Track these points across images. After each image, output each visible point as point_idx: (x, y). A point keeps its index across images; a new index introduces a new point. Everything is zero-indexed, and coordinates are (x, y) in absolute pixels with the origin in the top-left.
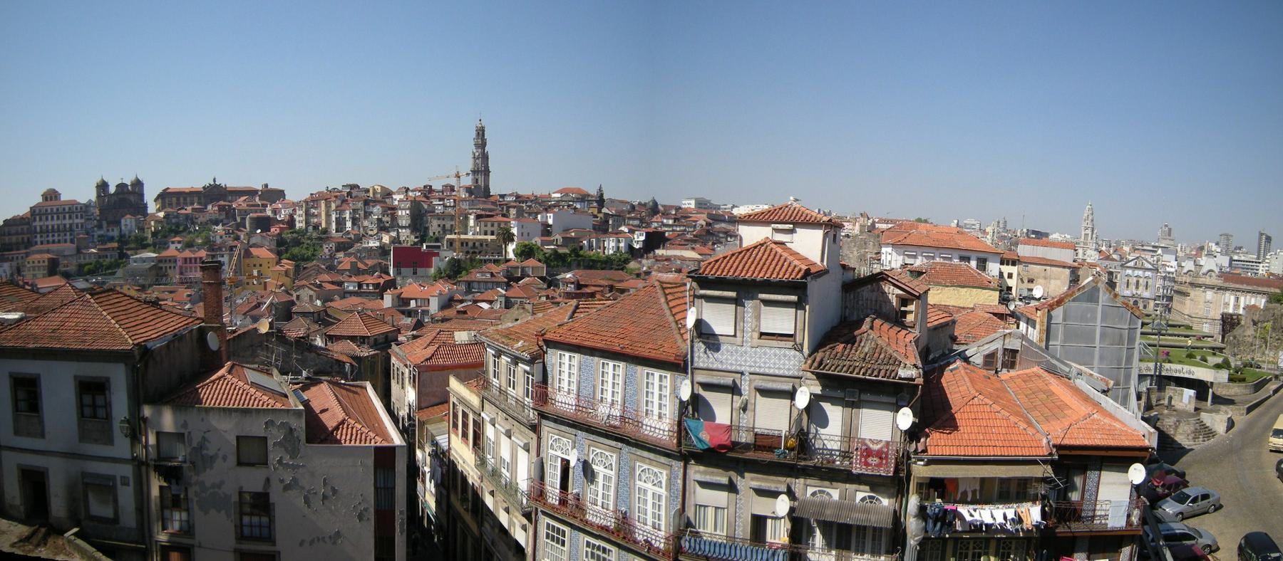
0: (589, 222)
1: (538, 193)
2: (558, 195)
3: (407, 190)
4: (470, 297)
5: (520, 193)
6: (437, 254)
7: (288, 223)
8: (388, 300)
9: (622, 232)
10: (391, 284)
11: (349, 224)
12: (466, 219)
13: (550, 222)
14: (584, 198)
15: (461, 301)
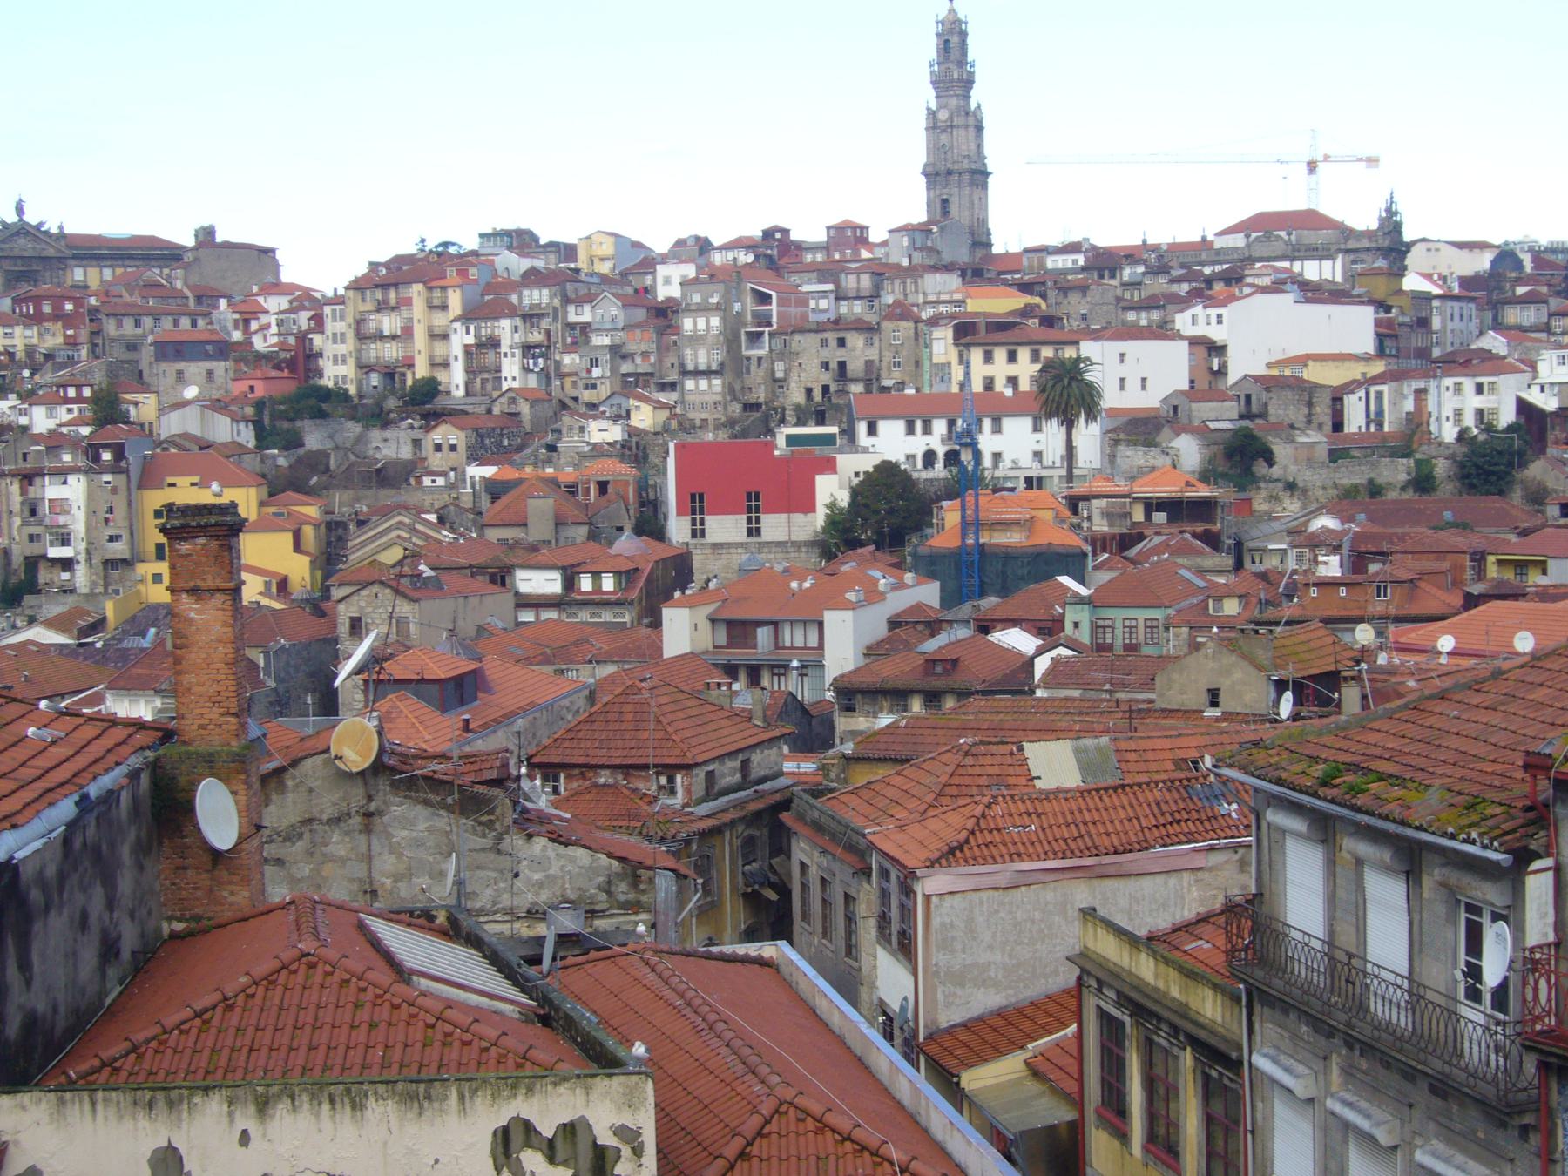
0: (1353, 329)
1: (1161, 236)
2: (1238, 241)
3: (704, 245)
4: (966, 610)
5: (1103, 240)
6: (829, 466)
7: (291, 364)
8: (682, 630)
9: (1487, 356)
10: (675, 575)
11: (511, 370)
12: (920, 340)
13: (1216, 334)
14: (1341, 240)
15: (934, 627)
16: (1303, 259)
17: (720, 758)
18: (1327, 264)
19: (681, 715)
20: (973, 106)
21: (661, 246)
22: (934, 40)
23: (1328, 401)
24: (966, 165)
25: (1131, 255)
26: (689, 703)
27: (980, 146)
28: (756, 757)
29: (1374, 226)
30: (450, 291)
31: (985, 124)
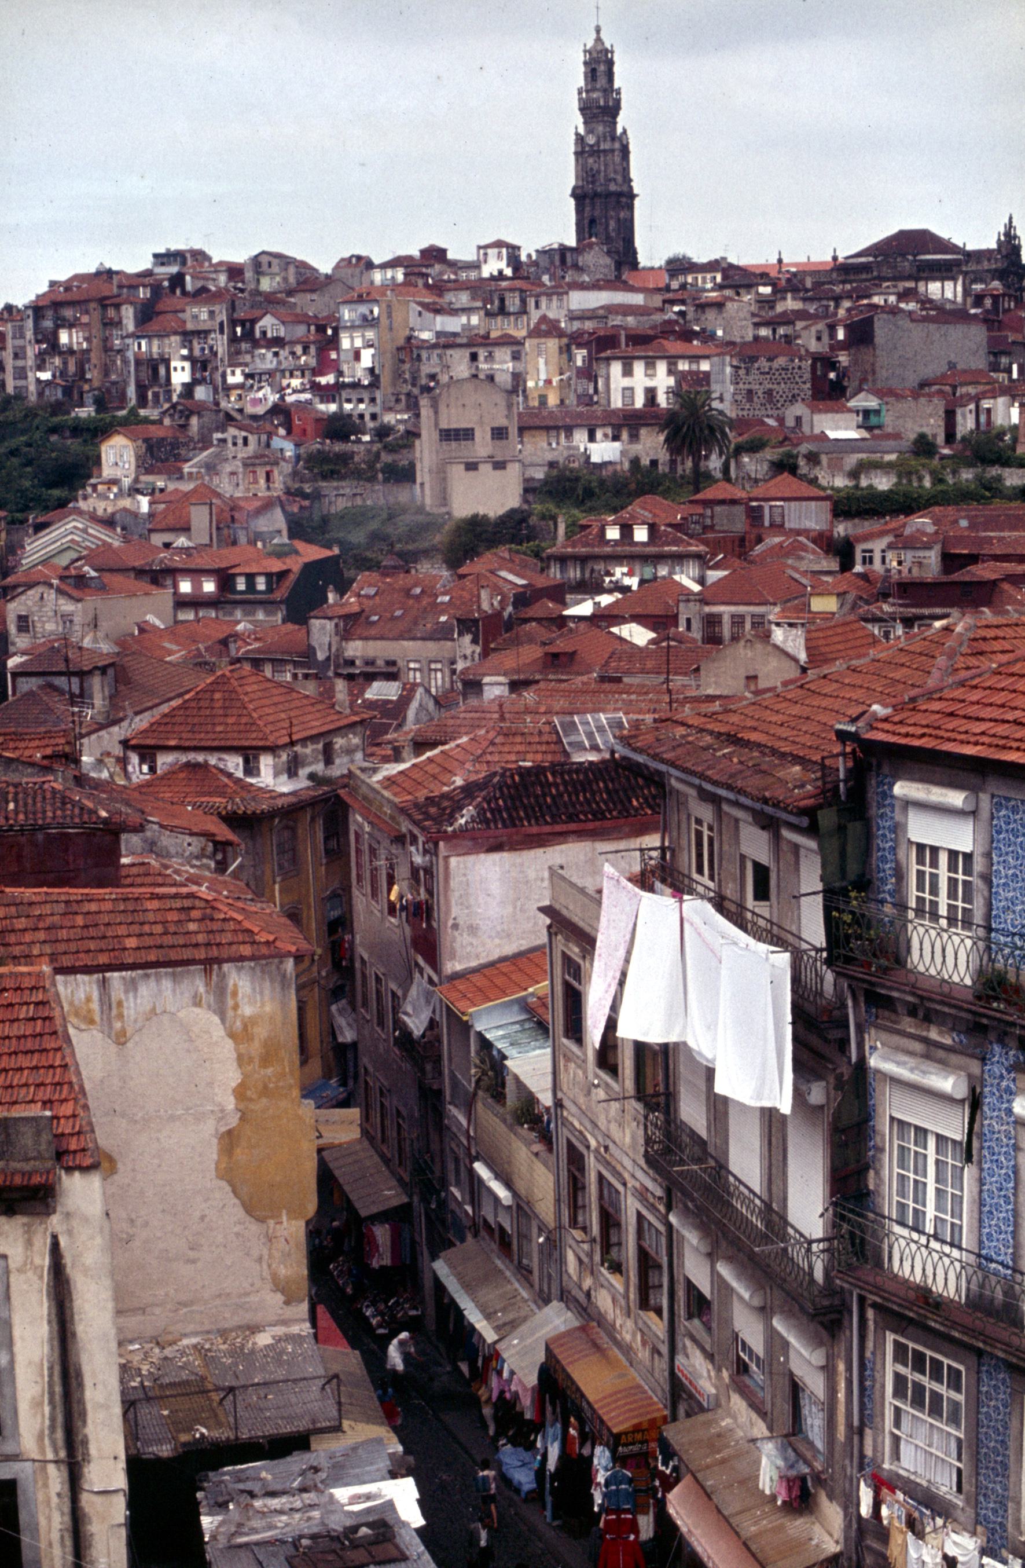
16: (927, 279)
17: (304, 741)
18: (949, 285)
19: (267, 702)
20: (619, 130)
21: (325, 266)
22: (582, 69)
23: (942, 413)
24: (613, 187)
25: (763, 276)
26: (275, 691)
27: (626, 170)
28: (339, 742)
29: (994, 246)
30: (124, 307)
31: (631, 148)
